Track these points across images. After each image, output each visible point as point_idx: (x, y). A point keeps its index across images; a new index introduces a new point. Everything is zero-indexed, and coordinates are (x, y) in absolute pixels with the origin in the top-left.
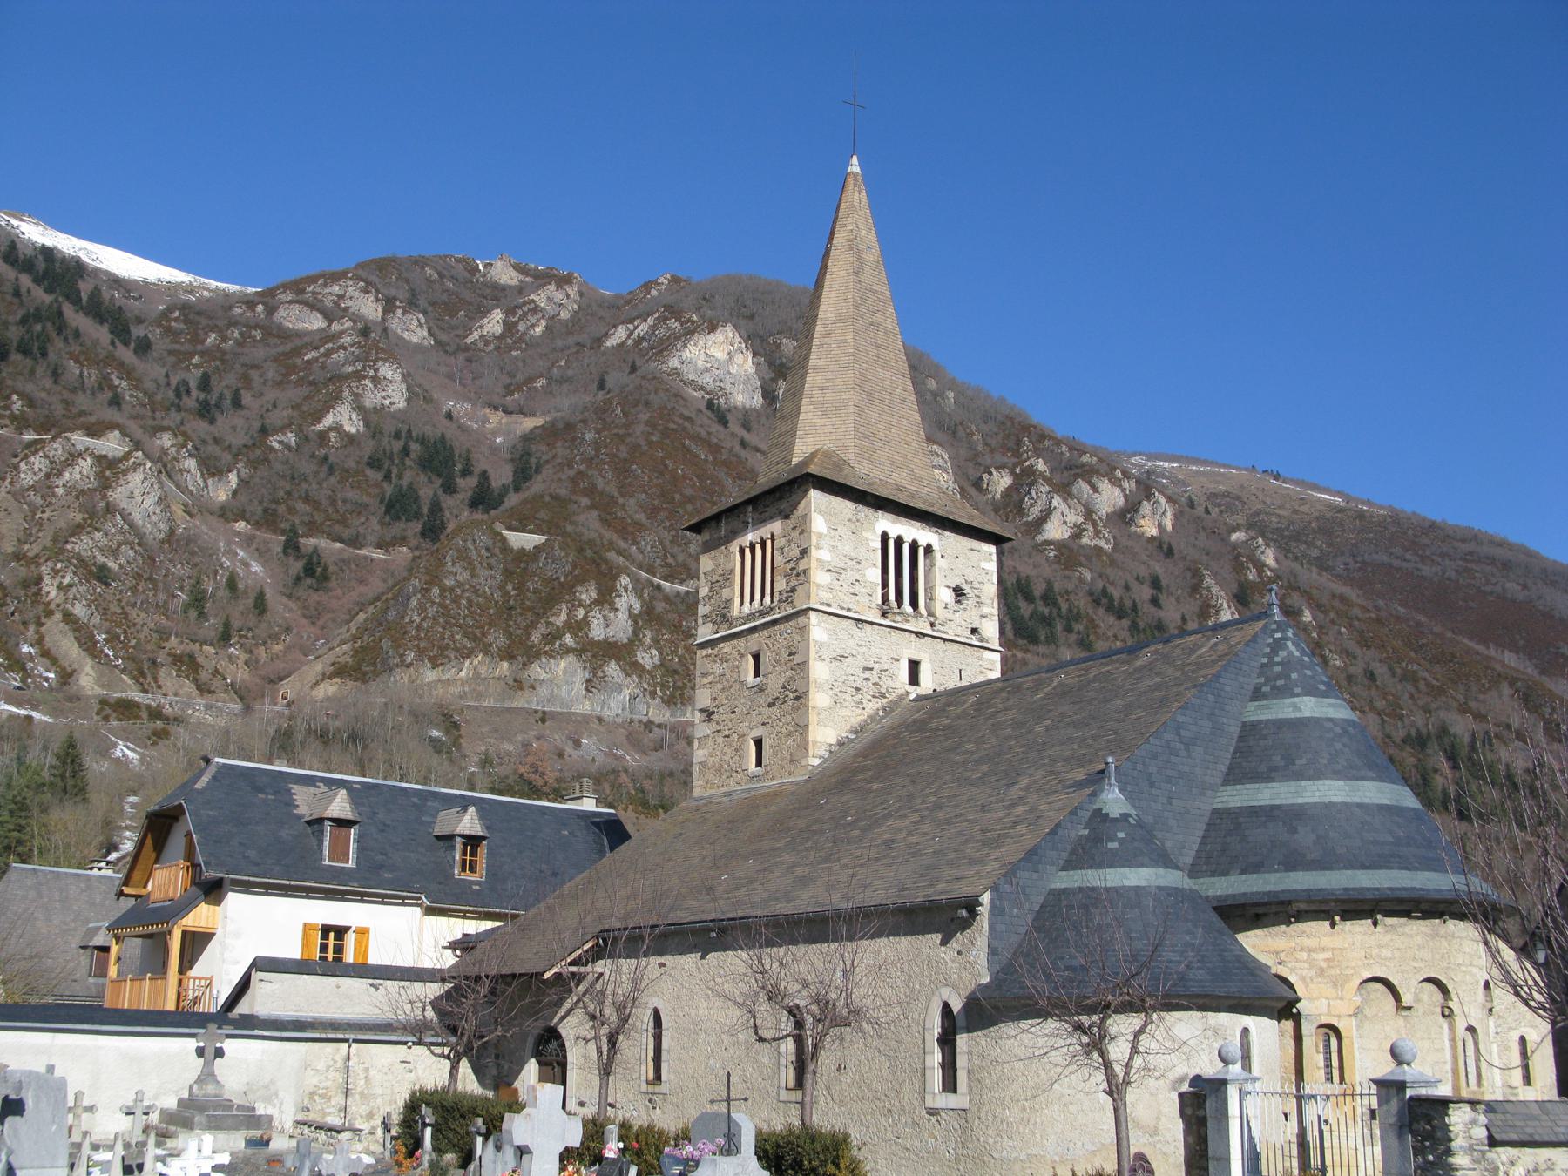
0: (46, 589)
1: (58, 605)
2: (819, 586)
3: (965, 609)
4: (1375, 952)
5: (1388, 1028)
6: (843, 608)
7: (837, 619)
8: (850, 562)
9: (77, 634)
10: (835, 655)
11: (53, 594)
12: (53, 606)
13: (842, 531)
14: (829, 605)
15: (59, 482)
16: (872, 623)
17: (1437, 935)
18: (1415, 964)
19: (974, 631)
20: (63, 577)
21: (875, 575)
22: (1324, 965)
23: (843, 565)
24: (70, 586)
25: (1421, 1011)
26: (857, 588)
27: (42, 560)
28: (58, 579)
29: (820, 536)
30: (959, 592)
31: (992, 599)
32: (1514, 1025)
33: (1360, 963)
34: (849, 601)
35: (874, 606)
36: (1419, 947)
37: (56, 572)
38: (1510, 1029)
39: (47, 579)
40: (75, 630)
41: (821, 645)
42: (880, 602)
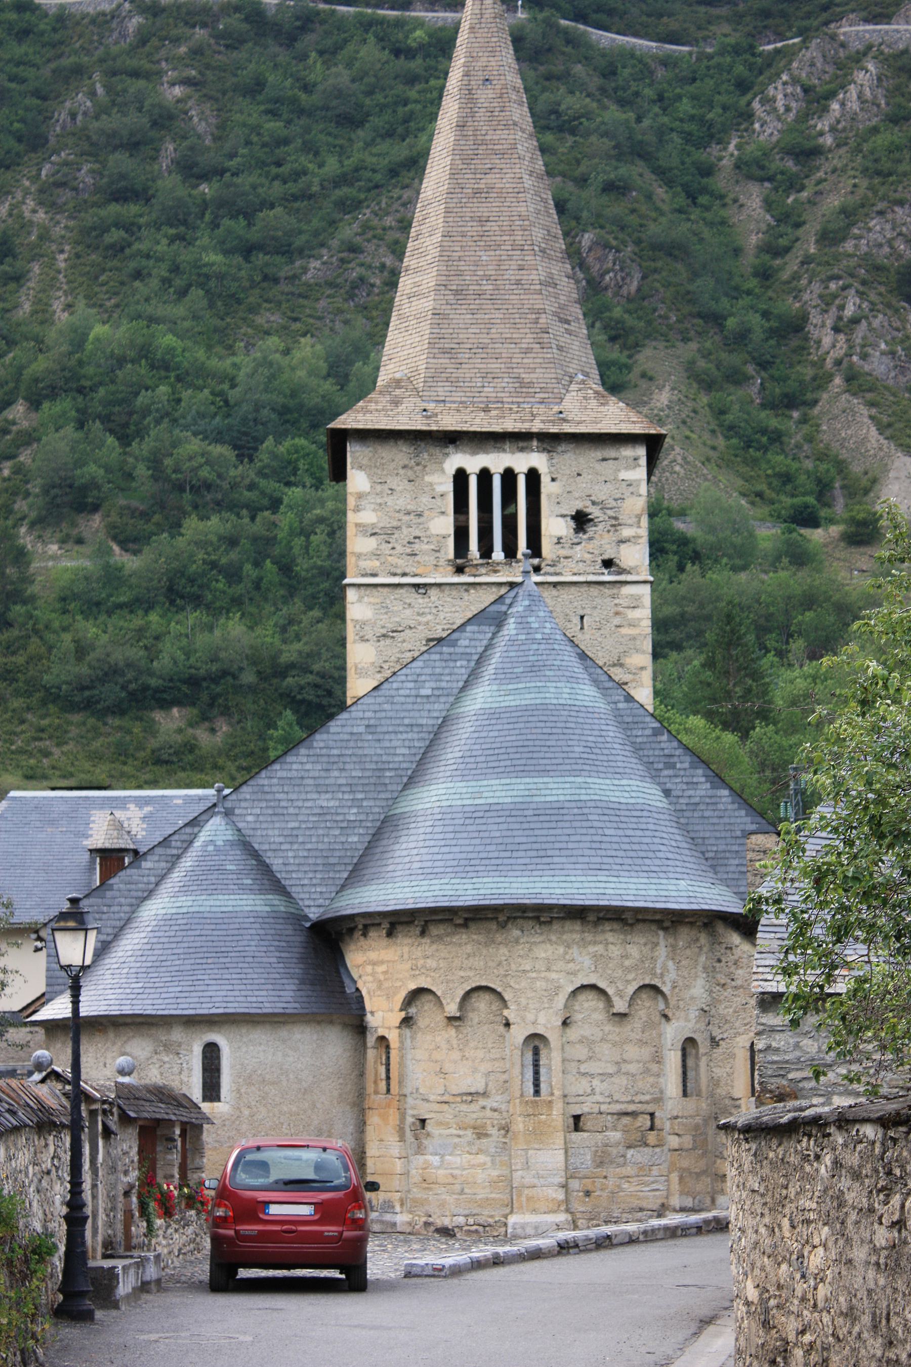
0: (815, 334)
1: (838, 363)
2: (359, 556)
3: (591, 539)
4: (421, 962)
5: (438, 1039)
6: (395, 575)
7: (386, 590)
8: (407, 518)
9: (874, 411)
10: (384, 631)
11: (827, 341)
12: (829, 362)
13: (393, 482)
14: (374, 575)
15: (823, 125)
16: (439, 585)
17: (493, 942)
18: (462, 973)
19: (608, 564)
20: (842, 308)
21: (445, 525)
22: (382, 977)
23: (395, 524)
24: (855, 321)
25: (476, 1020)
26: (417, 547)
27: (804, 282)
28: (833, 310)
29: (360, 496)
30: (581, 520)
31: (639, 517)
32: (741, 1030)
33: (407, 974)
34: (403, 564)
35: (442, 562)
36: (469, 956)
37: (827, 301)
38: (738, 1034)
39: (815, 318)
40: (872, 404)
41: (363, 624)
42: (451, 554)
